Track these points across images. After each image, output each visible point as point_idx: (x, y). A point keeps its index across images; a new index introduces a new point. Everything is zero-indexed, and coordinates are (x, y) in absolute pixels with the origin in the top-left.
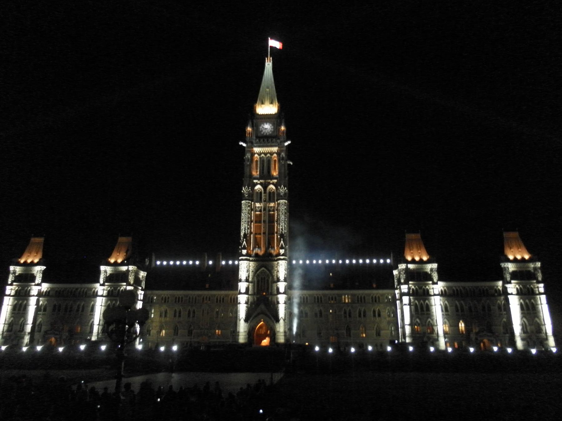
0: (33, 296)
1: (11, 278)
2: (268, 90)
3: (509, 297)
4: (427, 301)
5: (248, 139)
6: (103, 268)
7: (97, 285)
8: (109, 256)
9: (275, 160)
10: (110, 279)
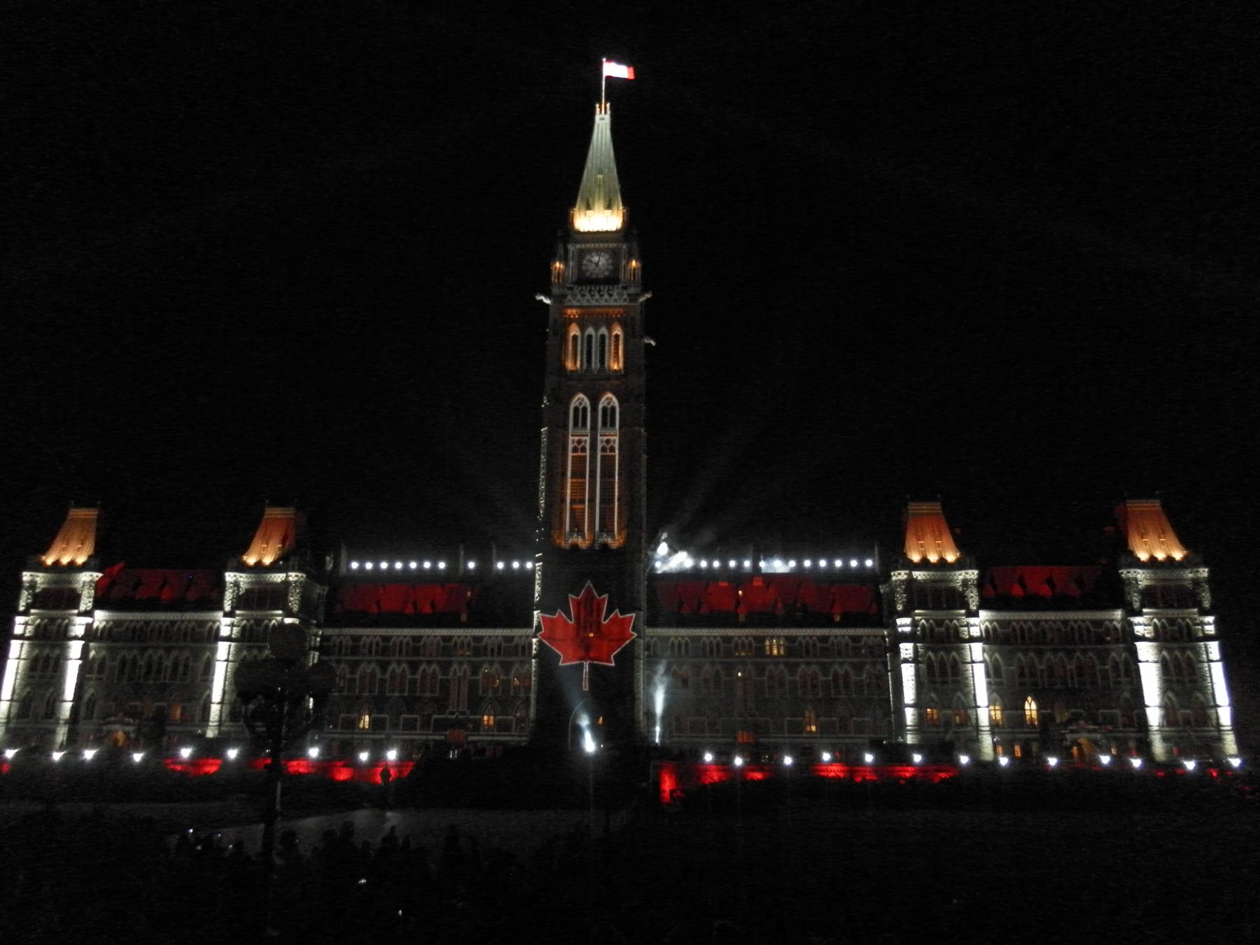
0: (76, 638)
1: (24, 600)
2: (600, 177)
3: (1139, 645)
5: (555, 290)
6: (230, 577)
7: (221, 614)
8: (245, 548)
9: (617, 336)
10: (242, 601)
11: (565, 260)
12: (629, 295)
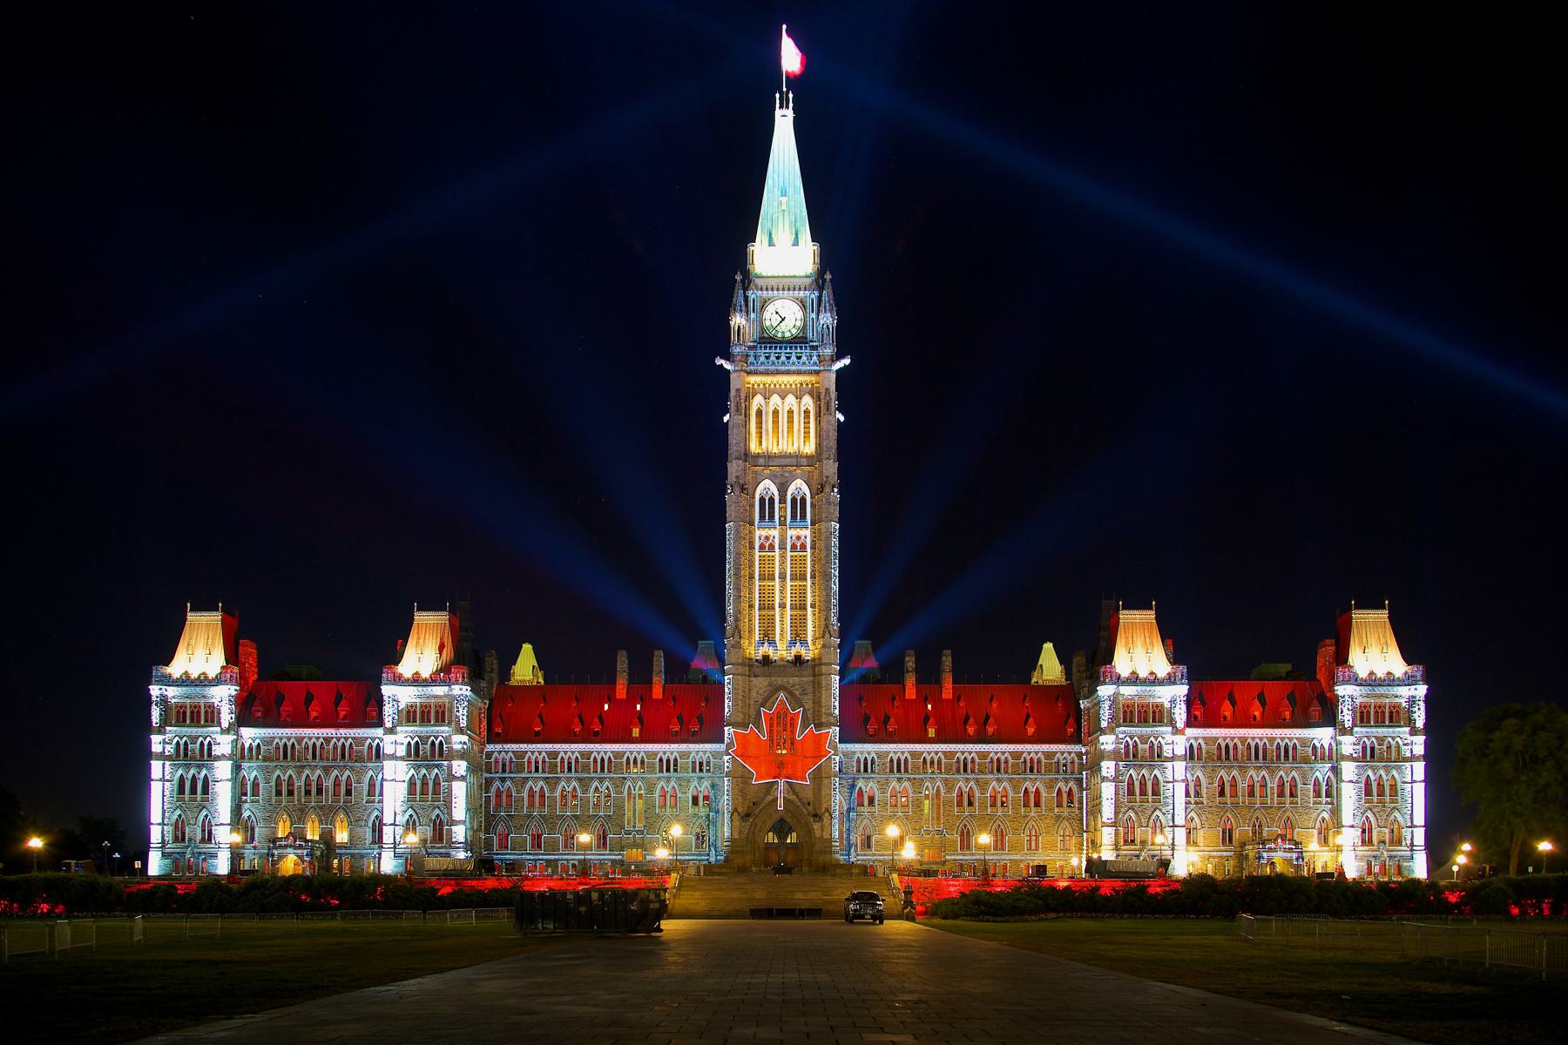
4: (1156, 772)
5: (736, 350)
7: (379, 732)
8: (396, 658)
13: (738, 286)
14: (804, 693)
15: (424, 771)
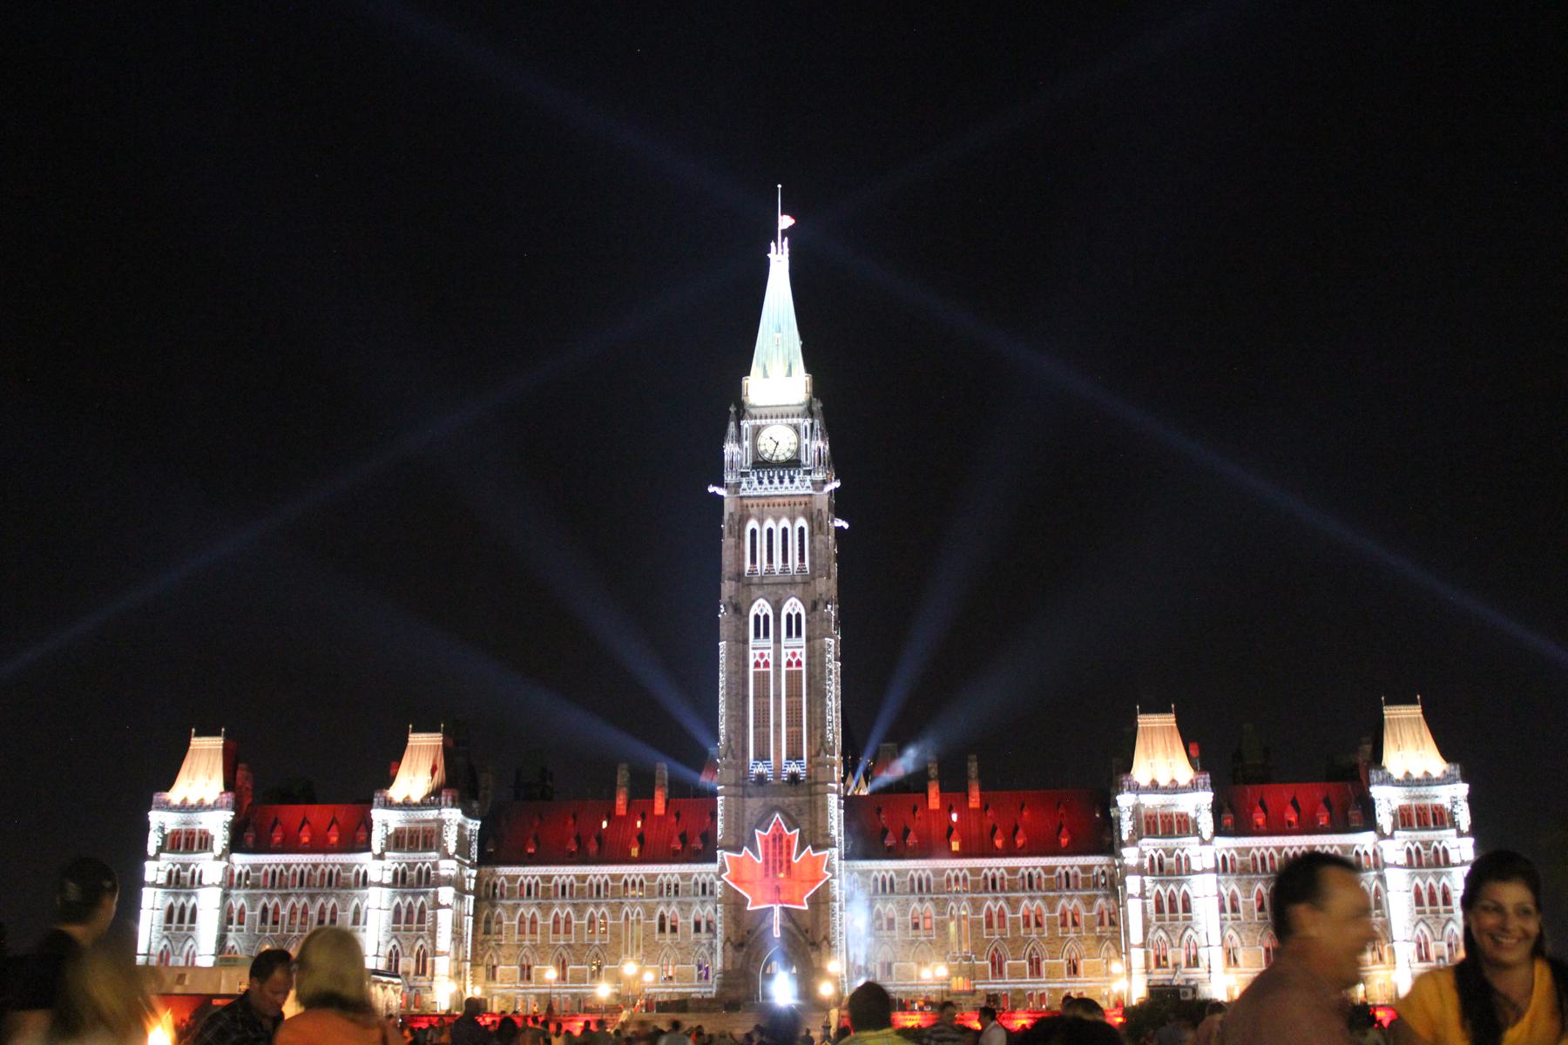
8: (388, 781)
10: (398, 841)
11: (739, 440)
12: (814, 483)
13: (733, 416)
14: (800, 812)
15: (409, 899)
